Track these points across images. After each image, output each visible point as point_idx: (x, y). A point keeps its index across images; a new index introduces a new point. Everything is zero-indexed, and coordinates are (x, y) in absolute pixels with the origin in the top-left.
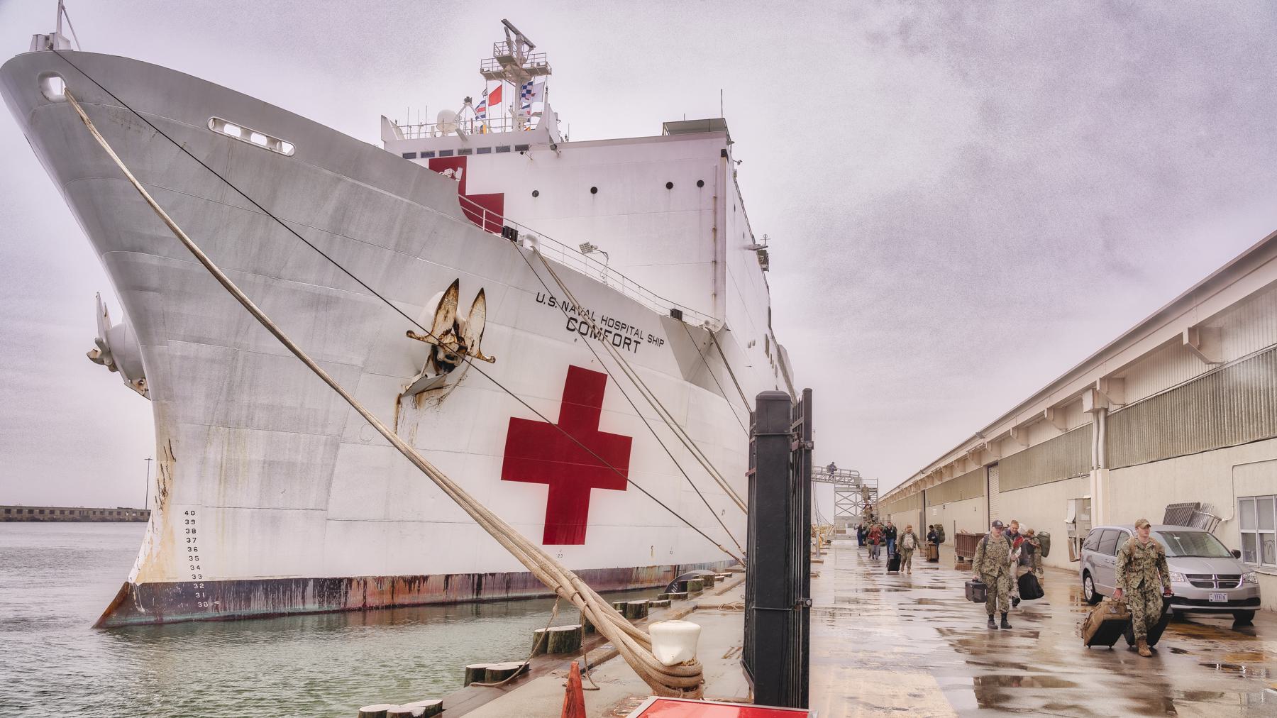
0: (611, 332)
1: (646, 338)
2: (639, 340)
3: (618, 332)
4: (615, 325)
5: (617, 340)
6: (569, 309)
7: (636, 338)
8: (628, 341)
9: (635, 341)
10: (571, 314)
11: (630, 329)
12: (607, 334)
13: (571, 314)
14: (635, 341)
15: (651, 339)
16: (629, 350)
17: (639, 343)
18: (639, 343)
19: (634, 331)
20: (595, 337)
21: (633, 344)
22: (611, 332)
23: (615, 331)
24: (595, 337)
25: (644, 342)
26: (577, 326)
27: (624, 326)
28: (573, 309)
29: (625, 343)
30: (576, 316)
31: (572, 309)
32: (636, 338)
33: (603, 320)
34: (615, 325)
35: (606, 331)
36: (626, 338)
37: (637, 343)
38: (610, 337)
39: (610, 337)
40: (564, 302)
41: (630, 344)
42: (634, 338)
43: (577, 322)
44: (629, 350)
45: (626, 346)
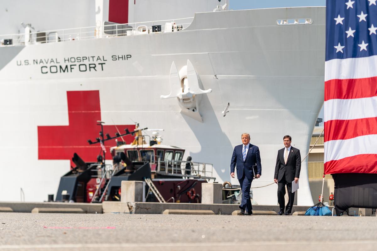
0: (75, 65)
1: (108, 58)
2: (103, 62)
3: (82, 63)
4: (76, 60)
5: (83, 68)
6: (38, 62)
7: (99, 61)
8: (94, 66)
9: (99, 64)
10: (42, 65)
11: (91, 59)
12: (72, 67)
13: (42, 65)
14: (99, 64)
15: (114, 58)
16: (96, 70)
17: (104, 64)
18: (104, 64)
19: (95, 59)
20: (64, 71)
21: (99, 67)
22: (75, 65)
23: (78, 64)
24: (64, 71)
25: (110, 63)
26: (48, 70)
27: (85, 58)
28: (41, 62)
29: (90, 68)
30: (45, 65)
31: (40, 62)
32: (99, 61)
33: (65, 60)
34: (76, 60)
35: (71, 66)
36: (90, 65)
37: (102, 64)
38: (76, 68)
39: (76, 68)
40: (34, 60)
41: (95, 67)
42: (97, 63)
43: (47, 67)
44: (96, 70)
45: (92, 69)
